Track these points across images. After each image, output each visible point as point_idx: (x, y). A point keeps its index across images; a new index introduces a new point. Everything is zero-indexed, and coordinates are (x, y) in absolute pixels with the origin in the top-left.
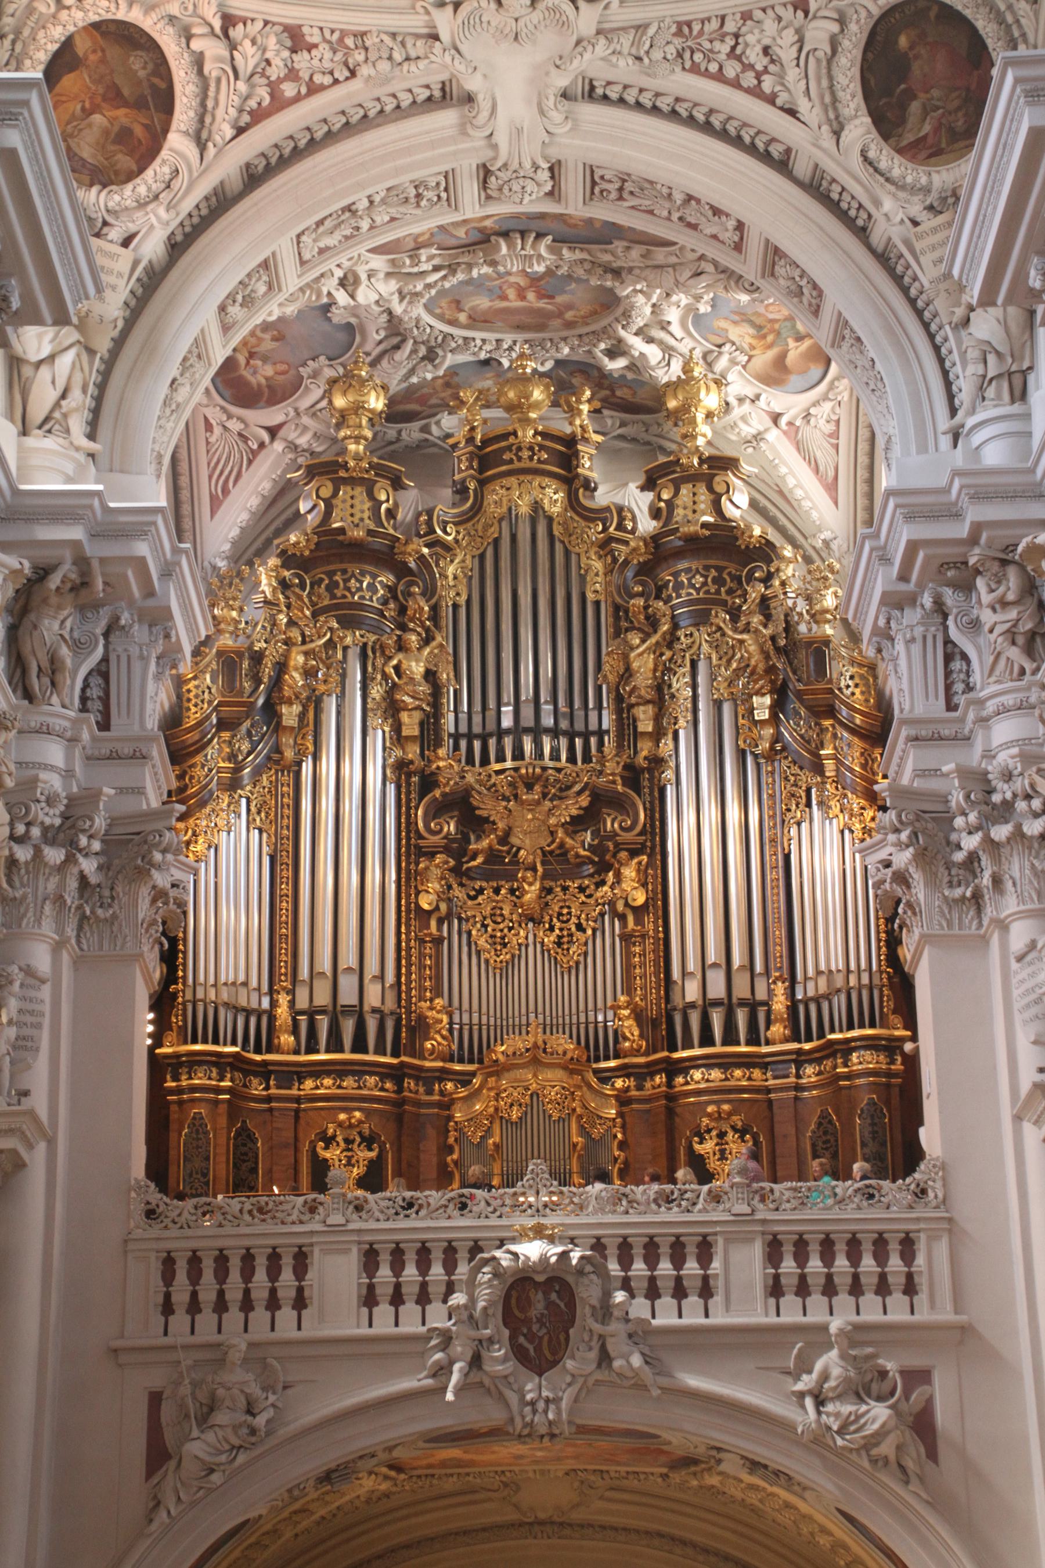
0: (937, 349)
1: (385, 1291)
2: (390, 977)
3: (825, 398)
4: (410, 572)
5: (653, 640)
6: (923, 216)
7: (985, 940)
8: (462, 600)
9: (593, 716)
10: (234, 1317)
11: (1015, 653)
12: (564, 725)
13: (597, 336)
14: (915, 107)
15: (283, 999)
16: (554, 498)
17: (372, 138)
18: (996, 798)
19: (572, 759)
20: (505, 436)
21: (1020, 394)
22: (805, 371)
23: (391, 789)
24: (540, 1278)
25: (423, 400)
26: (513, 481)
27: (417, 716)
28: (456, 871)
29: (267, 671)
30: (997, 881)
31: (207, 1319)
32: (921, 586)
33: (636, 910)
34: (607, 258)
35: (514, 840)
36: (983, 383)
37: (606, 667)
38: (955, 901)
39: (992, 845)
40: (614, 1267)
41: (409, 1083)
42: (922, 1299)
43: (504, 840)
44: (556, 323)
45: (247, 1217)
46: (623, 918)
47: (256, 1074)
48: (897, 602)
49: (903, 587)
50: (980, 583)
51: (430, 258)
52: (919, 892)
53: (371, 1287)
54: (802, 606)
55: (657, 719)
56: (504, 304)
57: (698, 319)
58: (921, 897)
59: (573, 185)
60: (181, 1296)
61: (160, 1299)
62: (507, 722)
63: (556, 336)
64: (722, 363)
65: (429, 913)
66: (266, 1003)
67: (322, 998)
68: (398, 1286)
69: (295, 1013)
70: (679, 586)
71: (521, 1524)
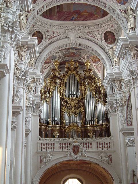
0: (111, 61)
1: (61, 147)
3: (99, 64)
4: (61, 79)
6: (110, 49)
7: (116, 115)
8: (66, 82)
10: (48, 149)
11: (119, 89)
14: (108, 40)
16: (75, 73)
17: (60, 41)
19: (76, 97)
21: (119, 65)
22: (97, 61)
28: (66, 108)
29: (49, 89)
31: (45, 149)
32: (110, 82)
34: (80, 51)
36: (116, 64)
39: (117, 106)
40: (83, 145)
41: (62, 128)
43: (70, 105)
46: (81, 112)
48: (108, 83)
57: (88, 57)
58: (111, 111)
59: (78, 45)
60: (43, 147)
64: (90, 61)
66: (48, 120)
67: (53, 120)
69: (51, 121)
70: (86, 81)
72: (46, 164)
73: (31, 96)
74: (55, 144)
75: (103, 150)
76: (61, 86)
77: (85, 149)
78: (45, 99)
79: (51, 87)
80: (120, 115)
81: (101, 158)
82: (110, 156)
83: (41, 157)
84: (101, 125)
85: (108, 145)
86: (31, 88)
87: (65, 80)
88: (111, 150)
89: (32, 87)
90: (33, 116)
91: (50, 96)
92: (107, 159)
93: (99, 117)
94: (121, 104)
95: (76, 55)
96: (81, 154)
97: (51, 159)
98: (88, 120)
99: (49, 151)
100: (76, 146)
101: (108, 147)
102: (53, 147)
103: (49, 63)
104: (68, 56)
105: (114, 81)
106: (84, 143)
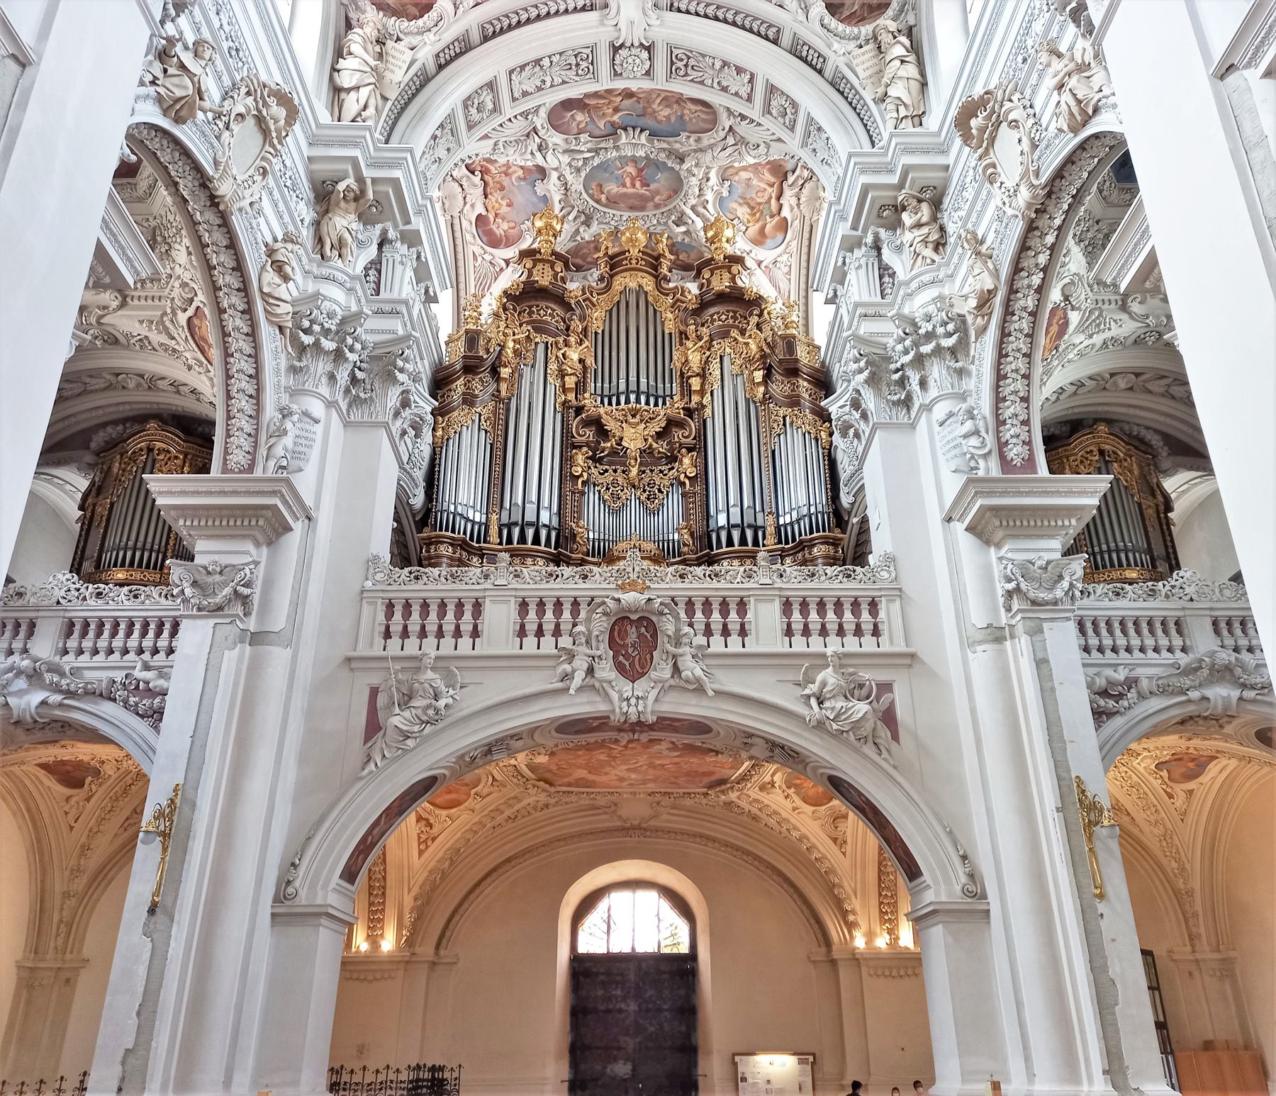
1: (531, 627)
2: (555, 509)
7: (913, 426)
9: (668, 385)
10: (431, 641)
11: (928, 252)
12: (652, 391)
15: (494, 517)
16: (648, 283)
18: (922, 331)
19: (656, 405)
20: (624, 253)
23: (559, 416)
24: (634, 617)
25: (584, 258)
26: (627, 274)
27: (574, 379)
30: (923, 384)
33: (689, 478)
34: (677, 146)
37: (675, 358)
38: (894, 403)
44: (650, 204)
45: (443, 579)
46: (683, 484)
47: (475, 554)
48: (850, 245)
49: (854, 233)
50: (905, 216)
52: (870, 400)
53: (522, 626)
54: (780, 322)
55: (703, 385)
56: (625, 190)
60: (396, 628)
61: (383, 628)
63: (650, 214)
66: (484, 520)
67: (517, 517)
68: (540, 626)
70: (713, 321)
71: (624, 829)
72: (410, 743)
73: (336, 293)
74: (488, 608)
75: (829, 651)
76: (567, 344)
77: (701, 640)
78: (469, 400)
79: (511, 344)
80: (940, 411)
81: (813, 702)
82: (886, 687)
83: (374, 692)
84: (802, 546)
85: (865, 616)
86: (340, 245)
87: (597, 318)
88: (886, 648)
89: (347, 235)
90: (347, 424)
91: (503, 393)
92: (862, 708)
93: (784, 506)
94: (950, 335)
96: (666, 673)
97: (441, 703)
98: (722, 520)
99: (433, 654)
100: (634, 617)
101: (867, 627)
102: (466, 627)
103: (509, 242)
104: (612, 202)
105: (891, 214)
106: (690, 603)
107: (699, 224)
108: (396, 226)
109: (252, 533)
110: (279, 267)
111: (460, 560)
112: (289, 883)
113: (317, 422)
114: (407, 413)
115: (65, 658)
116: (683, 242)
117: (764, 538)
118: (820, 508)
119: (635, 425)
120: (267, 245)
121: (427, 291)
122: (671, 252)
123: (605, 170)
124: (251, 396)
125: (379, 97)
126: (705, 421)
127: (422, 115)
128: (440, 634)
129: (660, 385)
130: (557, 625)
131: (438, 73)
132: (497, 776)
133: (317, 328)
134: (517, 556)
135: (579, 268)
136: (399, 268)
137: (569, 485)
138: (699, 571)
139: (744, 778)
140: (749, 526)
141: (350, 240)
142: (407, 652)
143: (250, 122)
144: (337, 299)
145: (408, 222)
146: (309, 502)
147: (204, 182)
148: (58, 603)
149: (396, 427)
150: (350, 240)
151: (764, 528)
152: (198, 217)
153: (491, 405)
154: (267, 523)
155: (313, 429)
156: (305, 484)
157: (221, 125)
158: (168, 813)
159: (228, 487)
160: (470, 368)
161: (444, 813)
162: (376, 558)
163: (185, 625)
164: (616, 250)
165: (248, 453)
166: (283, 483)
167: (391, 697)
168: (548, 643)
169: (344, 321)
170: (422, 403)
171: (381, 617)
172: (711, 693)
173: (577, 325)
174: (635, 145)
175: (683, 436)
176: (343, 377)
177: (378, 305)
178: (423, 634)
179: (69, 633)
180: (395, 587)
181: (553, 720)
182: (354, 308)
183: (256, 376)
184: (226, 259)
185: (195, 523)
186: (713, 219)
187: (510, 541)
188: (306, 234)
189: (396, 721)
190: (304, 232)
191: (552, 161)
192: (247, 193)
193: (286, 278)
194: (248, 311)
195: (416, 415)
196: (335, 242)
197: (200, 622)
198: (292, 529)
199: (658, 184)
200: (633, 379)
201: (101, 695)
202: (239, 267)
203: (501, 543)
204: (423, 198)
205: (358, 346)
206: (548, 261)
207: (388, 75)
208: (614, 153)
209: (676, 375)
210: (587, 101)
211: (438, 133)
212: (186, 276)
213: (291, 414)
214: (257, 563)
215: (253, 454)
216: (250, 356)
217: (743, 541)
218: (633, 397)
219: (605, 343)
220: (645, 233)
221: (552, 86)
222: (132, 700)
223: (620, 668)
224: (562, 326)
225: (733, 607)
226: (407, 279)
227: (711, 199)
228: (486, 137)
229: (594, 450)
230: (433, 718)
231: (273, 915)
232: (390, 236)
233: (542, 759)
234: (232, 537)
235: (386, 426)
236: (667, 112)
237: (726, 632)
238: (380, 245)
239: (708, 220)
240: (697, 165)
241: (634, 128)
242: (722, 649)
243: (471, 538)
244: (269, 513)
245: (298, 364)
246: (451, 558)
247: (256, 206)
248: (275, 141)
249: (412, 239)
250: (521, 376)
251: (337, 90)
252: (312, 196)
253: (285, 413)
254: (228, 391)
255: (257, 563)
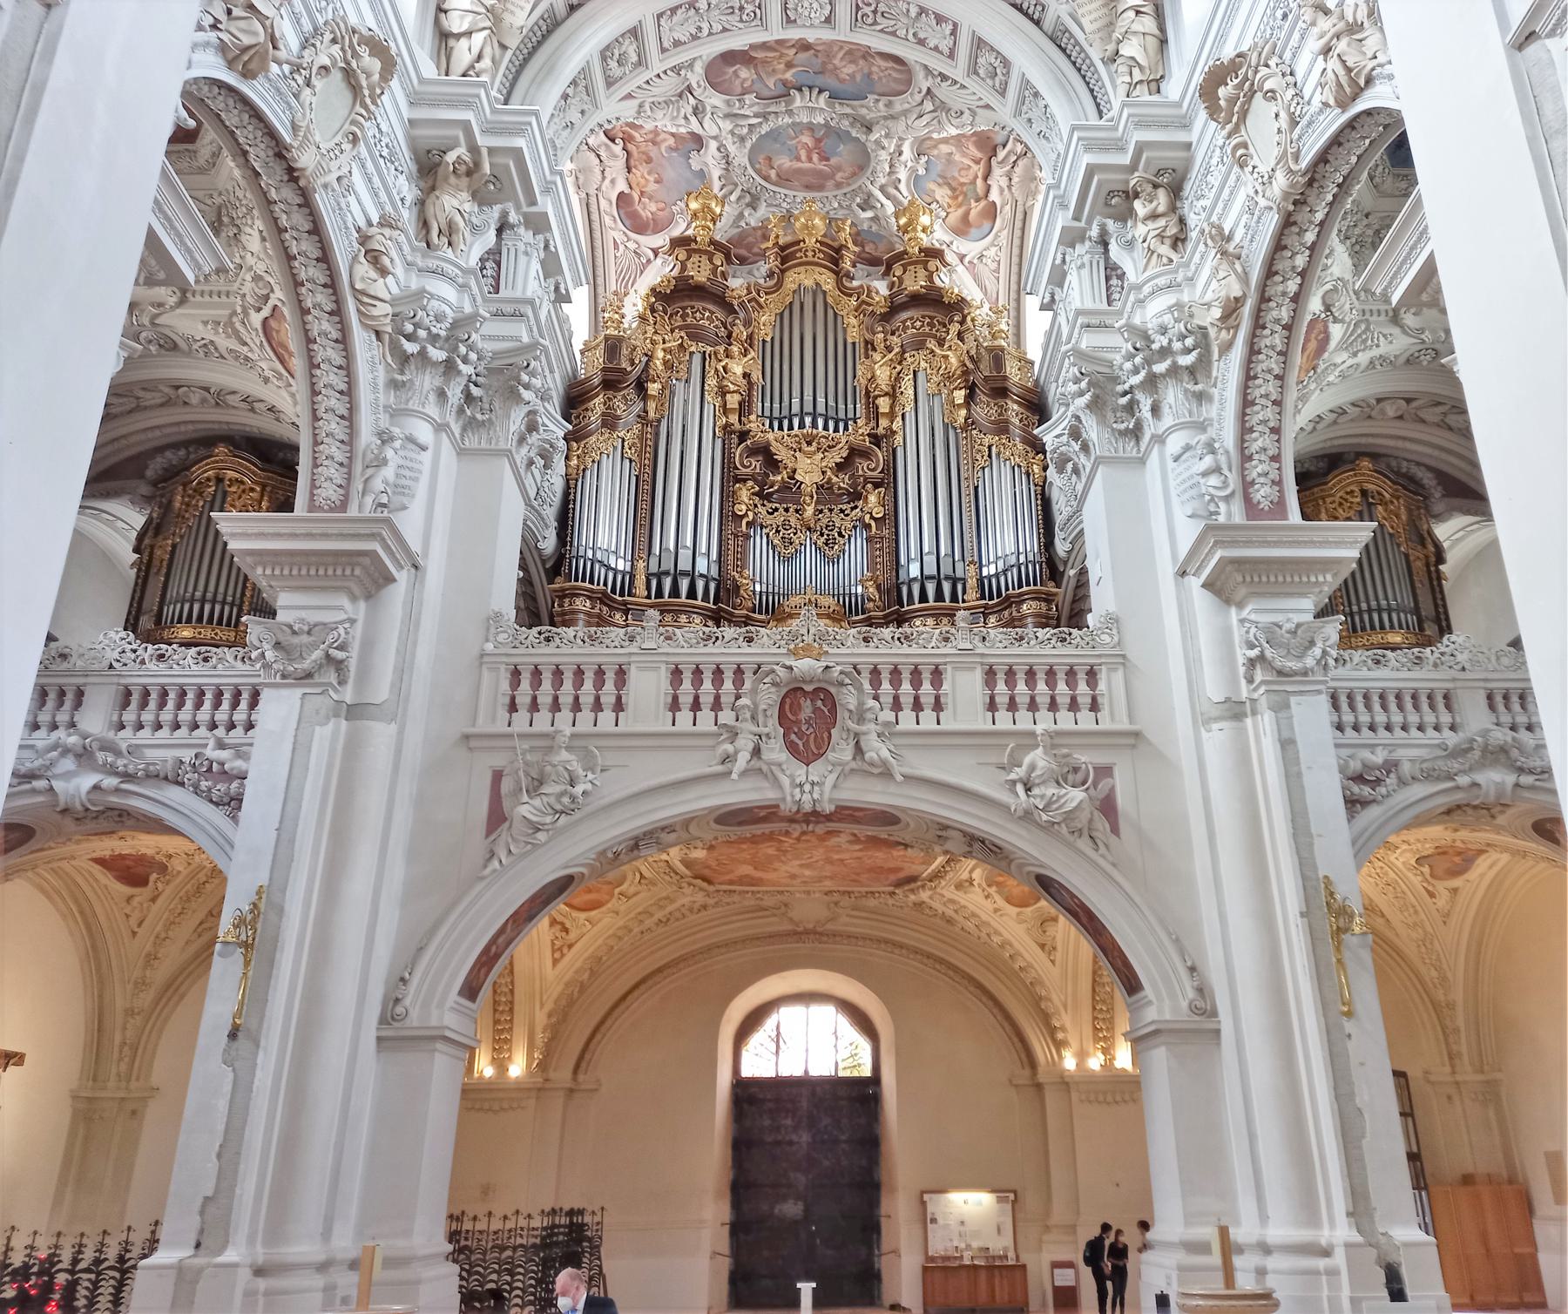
1: (686, 700)
2: (714, 556)
5: (890, 356)
9: (850, 406)
10: (565, 715)
12: (831, 413)
13: (855, 192)
15: (641, 565)
16: (827, 281)
19: (836, 430)
20: (798, 243)
23: (719, 442)
25: (749, 248)
26: (802, 269)
27: (737, 397)
35: (797, 477)
37: (859, 373)
40: (867, 686)
42: (1104, 715)
44: (830, 183)
46: (868, 527)
47: (618, 609)
51: (751, 106)
53: (675, 698)
55: (892, 407)
56: (800, 165)
60: (523, 699)
61: (507, 700)
62: (796, 409)
65: (742, 517)
66: (628, 569)
67: (668, 565)
70: (905, 328)
71: (796, 933)
72: (542, 836)
73: (448, 291)
74: (633, 675)
77: (888, 715)
79: (660, 354)
83: (498, 776)
86: (449, 231)
89: (458, 218)
90: (462, 452)
91: (652, 414)
93: (989, 554)
95: (839, 169)
98: (914, 571)
102: (608, 699)
104: (784, 179)
106: (875, 672)
107: (890, 208)
108: (518, 207)
109: (346, 584)
110: (374, 258)
111: (599, 616)
112: (397, 1001)
113: (424, 449)
114: (533, 439)
115: (122, 734)
116: (869, 232)
117: (964, 592)
118: (1031, 558)
119: (810, 455)
120: (359, 230)
121: (557, 289)
122: (855, 243)
123: (775, 140)
124: (342, 417)
125: (496, 45)
126: (894, 450)
127: (549, 69)
128: (576, 707)
129: (841, 406)
130: (717, 698)
131: (569, 15)
132: (646, 874)
133: (422, 333)
134: (669, 611)
135: (743, 261)
136: (522, 259)
137: (731, 527)
138: (886, 632)
139: (937, 876)
140: (947, 578)
141: (461, 224)
142: (536, 728)
143: (337, 76)
144: (447, 297)
145: (533, 203)
146: (415, 545)
147: (280, 152)
148: (111, 666)
149: (521, 455)
150: (461, 224)
151: (964, 580)
152: (273, 194)
153: (636, 428)
154: (365, 572)
155: (419, 458)
156: (410, 524)
157: (300, 81)
158: (249, 920)
159: (316, 528)
160: (611, 382)
161: (583, 915)
162: (498, 616)
163: (266, 695)
164: (789, 239)
165: (340, 486)
166: (383, 525)
167: (518, 782)
168: (706, 716)
169: (455, 325)
170: (552, 427)
171: (505, 686)
172: (899, 778)
173: (741, 331)
174: (811, 109)
175: (868, 470)
176: (455, 393)
177: (498, 305)
178: (556, 706)
179: (126, 704)
180: (522, 650)
181: (712, 810)
182: (468, 309)
183: (349, 393)
184: (308, 246)
185: (277, 572)
186: (906, 202)
187: (659, 594)
188: (407, 216)
189: (524, 810)
190: (406, 214)
191: (710, 128)
192: (334, 165)
193: (384, 272)
194: (338, 312)
195: (544, 441)
196: (444, 227)
197: (285, 692)
198: (394, 580)
199: (839, 159)
200: (808, 398)
201: (166, 778)
202: (325, 258)
203: (649, 597)
204: (553, 172)
205: (473, 356)
206: (706, 252)
207: (507, 17)
208: (787, 120)
209: (861, 393)
210: (754, 54)
211: (570, 91)
212: (260, 268)
213: (392, 439)
214: (353, 621)
215: (346, 487)
216: (340, 368)
217: (939, 596)
218: (808, 420)
219: (774, 353)
220: (823, 219)
221: (710, 34)
222: (204, 784)
223: (792, 748)
224: (723, 332)
225: (926, 677)
226: (533, 274)
227: (904, 178)
228: (629, 96)
229: (762, 485)
230: (567, 809)
231: (379, 1039)
232: (511, 220)
233: (699, 854)
234: (323, 589)
235: (508, 454)
236: (850, 69)
237: (917, 706)
238: (500, 231)
239: (900, 203)
240: (887, 136)
241: (810, 88)
242: (913, 726)
243: (614, 590)
244: (366, 561)
245: (399, 377)
246: (588, 614)
247: (345, 181)
248: (368, 101)
249: (538, 224)
250: (672, 393)
251: (444, 37)
252: (414, 168)
253: (385, 438)
254: (314, 411)
255: (353, 621)
